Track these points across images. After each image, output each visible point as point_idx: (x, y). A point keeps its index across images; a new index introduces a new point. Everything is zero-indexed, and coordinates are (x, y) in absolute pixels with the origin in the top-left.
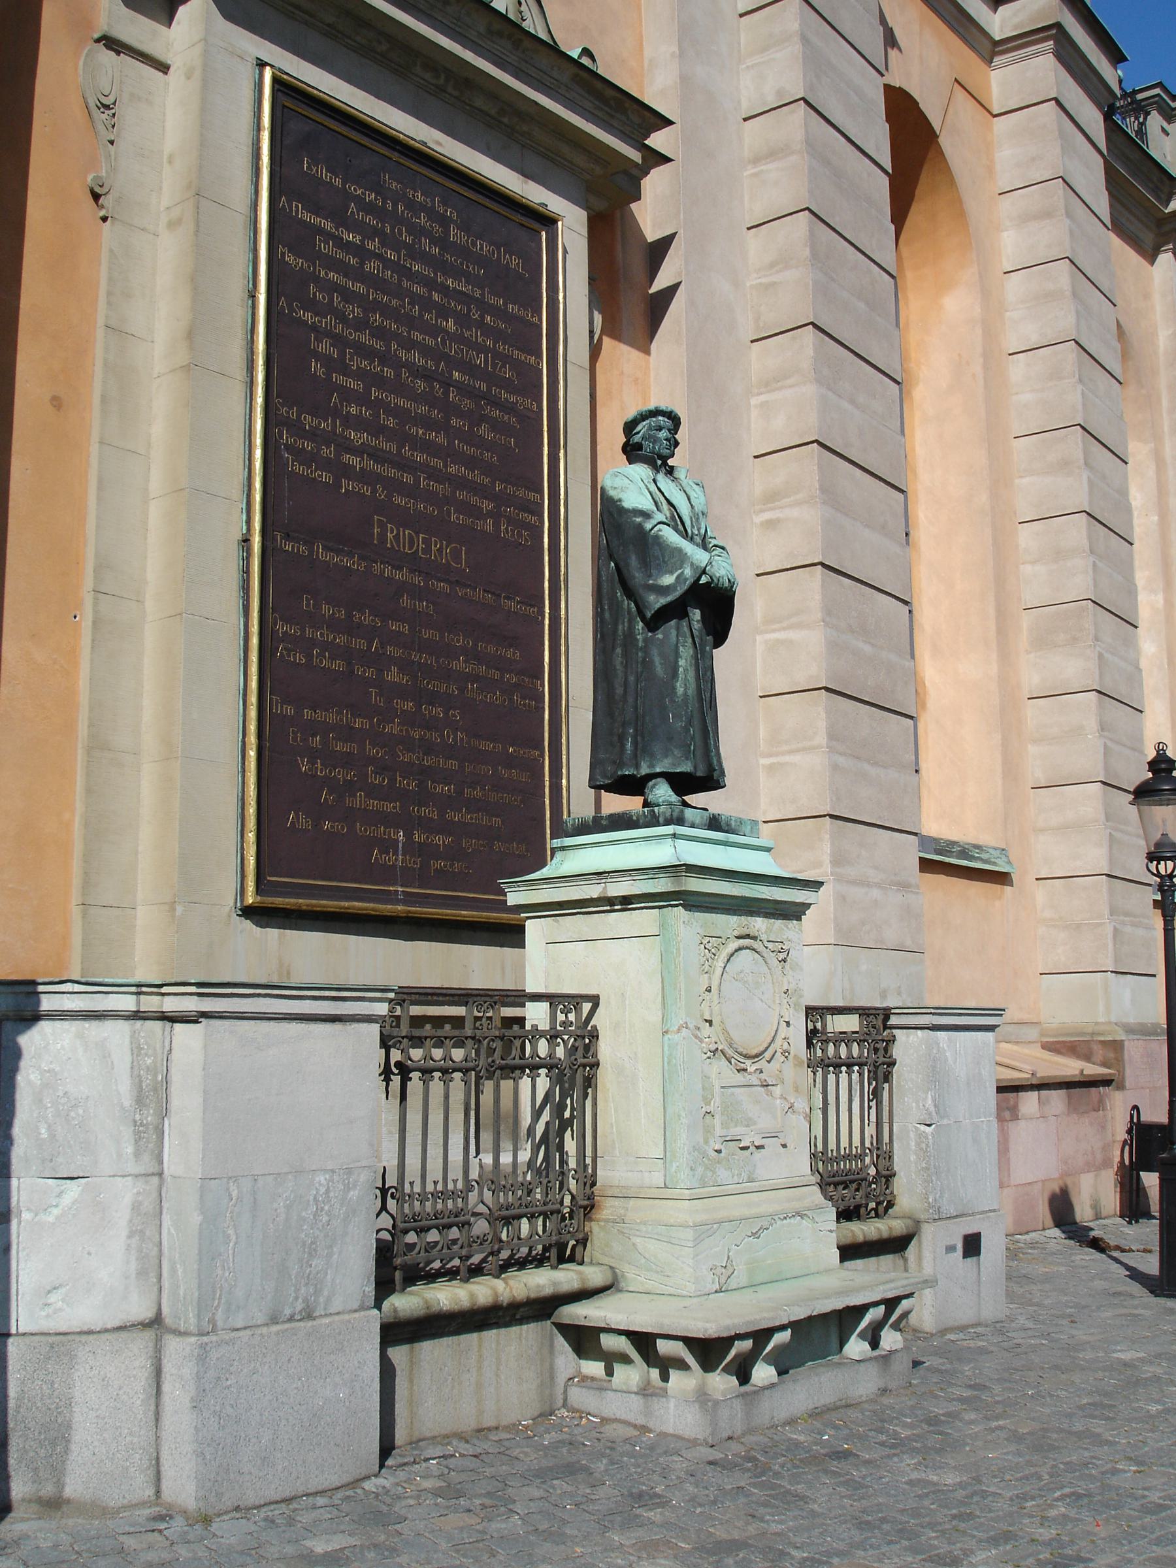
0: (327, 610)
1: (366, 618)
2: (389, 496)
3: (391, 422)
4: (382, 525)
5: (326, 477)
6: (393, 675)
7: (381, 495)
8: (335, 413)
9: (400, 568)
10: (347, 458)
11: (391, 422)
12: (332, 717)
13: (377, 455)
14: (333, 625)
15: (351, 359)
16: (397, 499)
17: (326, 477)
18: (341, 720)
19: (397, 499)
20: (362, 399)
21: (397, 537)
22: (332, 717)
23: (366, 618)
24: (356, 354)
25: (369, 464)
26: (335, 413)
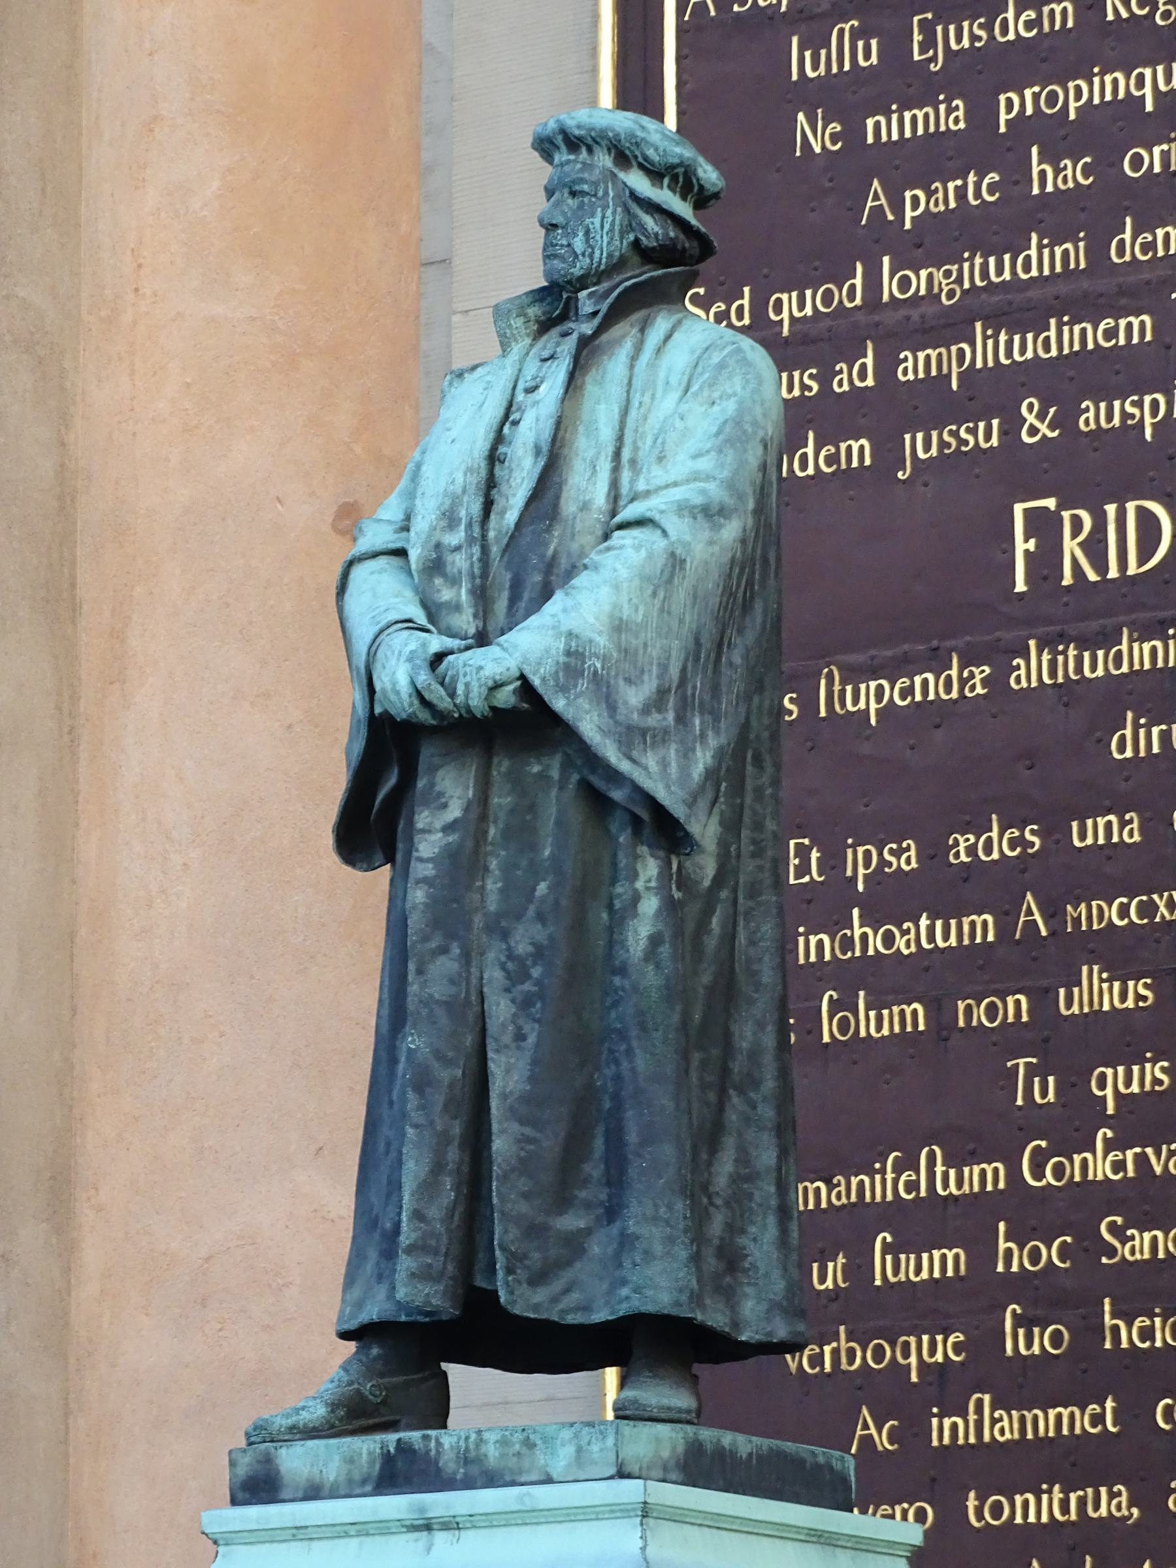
0: (859, 863)
1: (999, 843)
2: (1066, 421)
3: (1075, 173)
4: (1044, 527)
5: (859, 450)
6: (1098, 992)
7: (1036, 424)
8: (884, 238)
9: (1109, 639)
10: (912, 366)
11: (1075, 173)
12: (884, 1184)
13: (1017, 309)
14: (890, 901)
15: (928, 43)
16: (1092, 416)
17: (859, 450)
18: (912, 1186)
19: (1092, 416)
20: (979, 147)
21: (1095, 548)
22: (884, 1184)
23: (999, 843)
24: (938, 19)
25: (986, 349)
26: (884, 238)
